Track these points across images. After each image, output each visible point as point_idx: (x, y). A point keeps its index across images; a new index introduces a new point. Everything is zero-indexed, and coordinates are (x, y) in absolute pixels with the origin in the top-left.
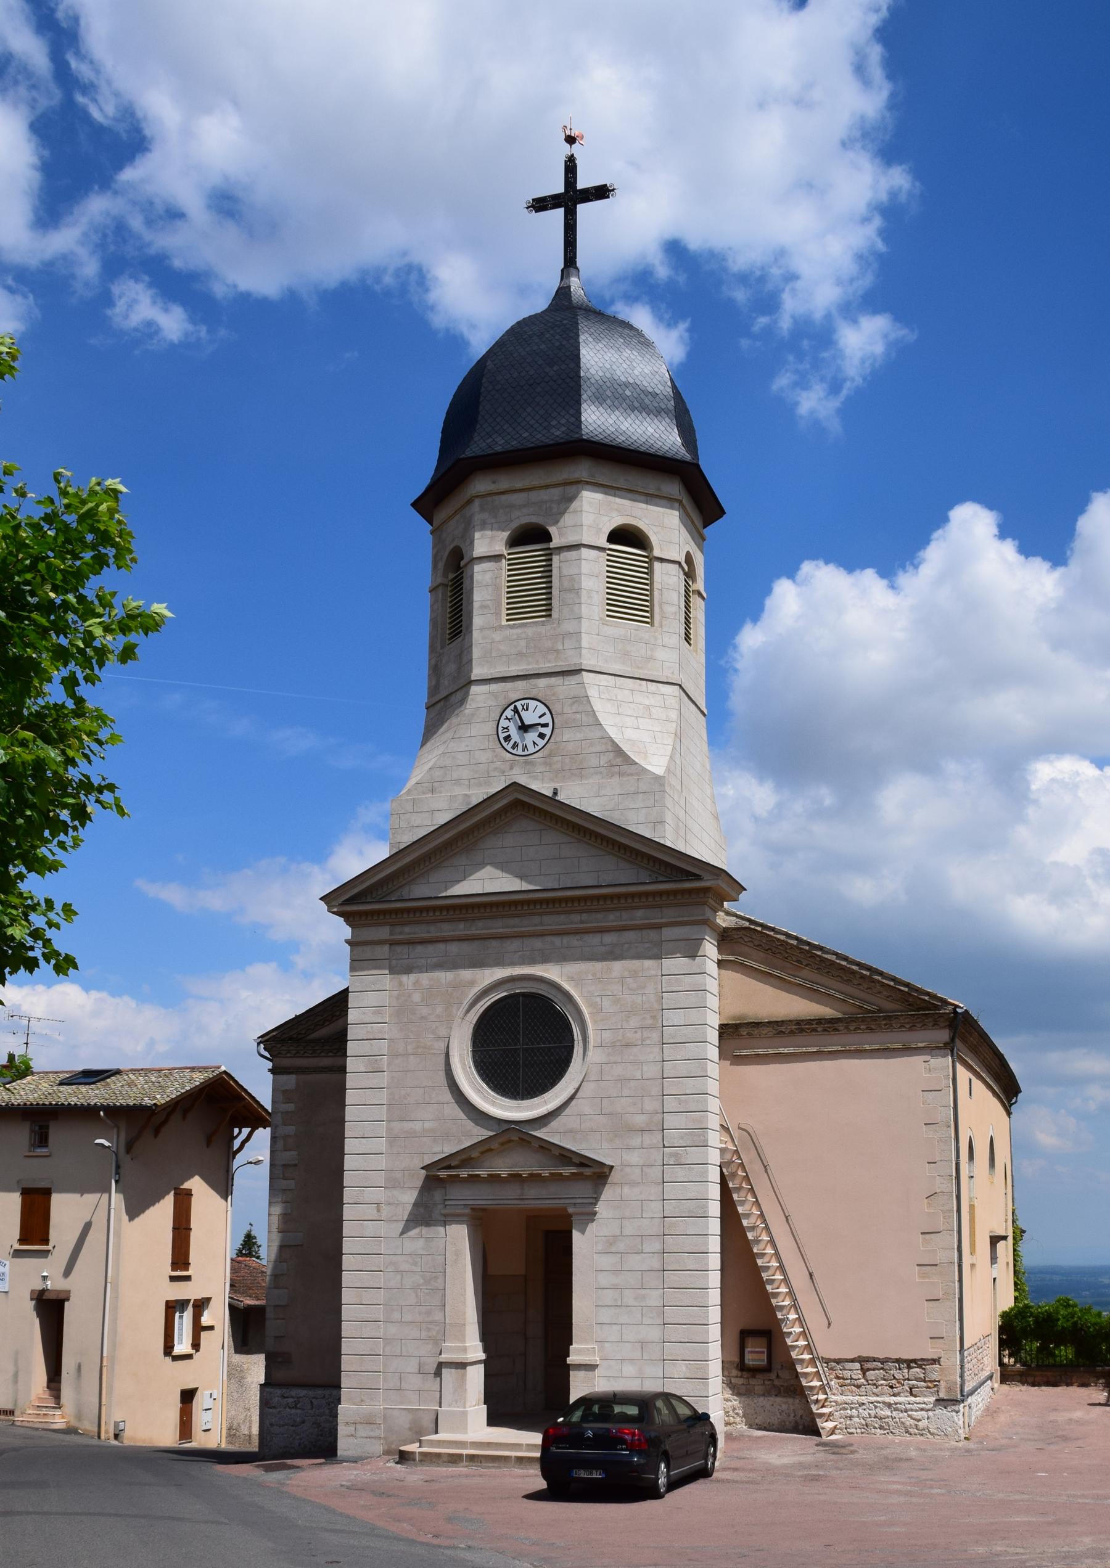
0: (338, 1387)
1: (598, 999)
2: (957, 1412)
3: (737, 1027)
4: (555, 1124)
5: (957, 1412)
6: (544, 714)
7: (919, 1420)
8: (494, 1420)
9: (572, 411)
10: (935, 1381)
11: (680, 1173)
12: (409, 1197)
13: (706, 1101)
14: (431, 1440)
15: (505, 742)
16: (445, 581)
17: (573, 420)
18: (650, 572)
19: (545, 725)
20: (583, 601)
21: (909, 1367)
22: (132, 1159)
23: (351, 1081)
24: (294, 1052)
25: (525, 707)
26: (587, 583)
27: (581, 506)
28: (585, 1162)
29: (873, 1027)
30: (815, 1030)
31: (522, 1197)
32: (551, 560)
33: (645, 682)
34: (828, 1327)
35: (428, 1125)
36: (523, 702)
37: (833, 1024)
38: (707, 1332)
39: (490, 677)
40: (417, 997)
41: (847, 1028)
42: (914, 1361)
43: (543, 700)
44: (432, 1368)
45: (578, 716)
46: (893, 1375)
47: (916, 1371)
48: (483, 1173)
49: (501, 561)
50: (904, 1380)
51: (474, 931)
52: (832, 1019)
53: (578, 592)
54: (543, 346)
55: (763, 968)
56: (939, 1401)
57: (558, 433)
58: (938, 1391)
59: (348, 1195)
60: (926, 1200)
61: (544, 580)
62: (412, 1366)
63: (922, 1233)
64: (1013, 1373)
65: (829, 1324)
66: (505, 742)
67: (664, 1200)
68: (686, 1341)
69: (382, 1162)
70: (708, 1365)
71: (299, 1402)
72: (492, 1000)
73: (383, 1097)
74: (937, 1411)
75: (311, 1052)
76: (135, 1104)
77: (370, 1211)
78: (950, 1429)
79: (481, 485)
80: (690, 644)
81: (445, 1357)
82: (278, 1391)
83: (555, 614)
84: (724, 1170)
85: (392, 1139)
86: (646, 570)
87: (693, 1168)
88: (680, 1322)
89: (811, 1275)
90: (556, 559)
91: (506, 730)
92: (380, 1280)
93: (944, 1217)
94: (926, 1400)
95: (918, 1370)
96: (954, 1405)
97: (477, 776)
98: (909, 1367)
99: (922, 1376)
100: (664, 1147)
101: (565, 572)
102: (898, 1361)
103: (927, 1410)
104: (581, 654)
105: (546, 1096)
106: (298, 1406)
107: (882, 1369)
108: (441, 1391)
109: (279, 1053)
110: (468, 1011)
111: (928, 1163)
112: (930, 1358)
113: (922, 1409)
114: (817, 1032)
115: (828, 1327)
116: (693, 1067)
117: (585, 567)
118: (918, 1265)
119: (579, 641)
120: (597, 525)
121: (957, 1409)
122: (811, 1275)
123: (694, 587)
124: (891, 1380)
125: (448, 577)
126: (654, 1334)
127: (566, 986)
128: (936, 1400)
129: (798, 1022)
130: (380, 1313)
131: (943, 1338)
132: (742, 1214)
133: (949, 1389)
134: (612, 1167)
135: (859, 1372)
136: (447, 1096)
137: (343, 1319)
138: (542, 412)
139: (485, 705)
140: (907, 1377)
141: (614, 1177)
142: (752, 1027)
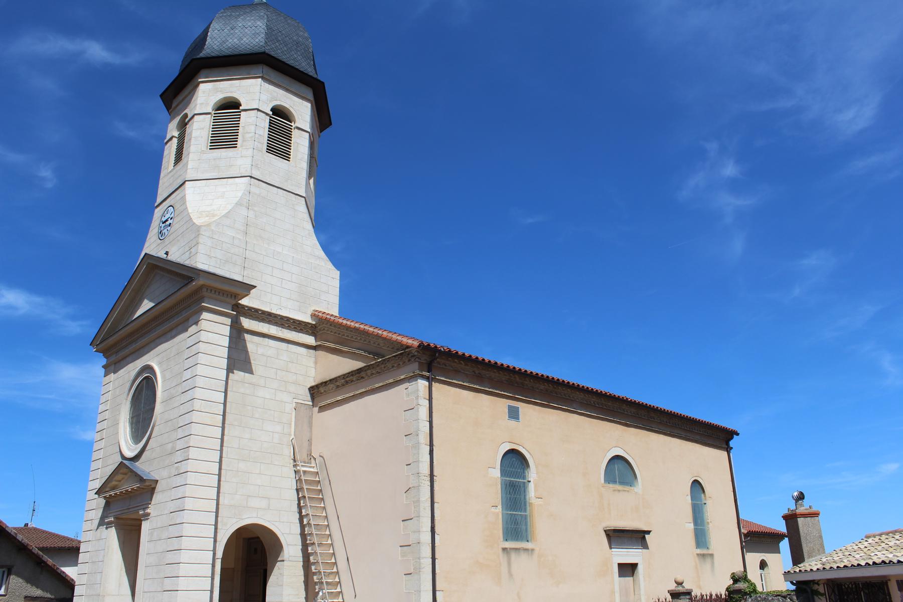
29: (379, 371)
30: (352, 381)
31: (129, 507)
52: (358, 370)
55: (332, 345)
60: (405, 494)
65: (356, 596)
93: (415, 508)
110: (128, 395)
111: (407, 465)
118: (401, 546)
141: (159, 487)
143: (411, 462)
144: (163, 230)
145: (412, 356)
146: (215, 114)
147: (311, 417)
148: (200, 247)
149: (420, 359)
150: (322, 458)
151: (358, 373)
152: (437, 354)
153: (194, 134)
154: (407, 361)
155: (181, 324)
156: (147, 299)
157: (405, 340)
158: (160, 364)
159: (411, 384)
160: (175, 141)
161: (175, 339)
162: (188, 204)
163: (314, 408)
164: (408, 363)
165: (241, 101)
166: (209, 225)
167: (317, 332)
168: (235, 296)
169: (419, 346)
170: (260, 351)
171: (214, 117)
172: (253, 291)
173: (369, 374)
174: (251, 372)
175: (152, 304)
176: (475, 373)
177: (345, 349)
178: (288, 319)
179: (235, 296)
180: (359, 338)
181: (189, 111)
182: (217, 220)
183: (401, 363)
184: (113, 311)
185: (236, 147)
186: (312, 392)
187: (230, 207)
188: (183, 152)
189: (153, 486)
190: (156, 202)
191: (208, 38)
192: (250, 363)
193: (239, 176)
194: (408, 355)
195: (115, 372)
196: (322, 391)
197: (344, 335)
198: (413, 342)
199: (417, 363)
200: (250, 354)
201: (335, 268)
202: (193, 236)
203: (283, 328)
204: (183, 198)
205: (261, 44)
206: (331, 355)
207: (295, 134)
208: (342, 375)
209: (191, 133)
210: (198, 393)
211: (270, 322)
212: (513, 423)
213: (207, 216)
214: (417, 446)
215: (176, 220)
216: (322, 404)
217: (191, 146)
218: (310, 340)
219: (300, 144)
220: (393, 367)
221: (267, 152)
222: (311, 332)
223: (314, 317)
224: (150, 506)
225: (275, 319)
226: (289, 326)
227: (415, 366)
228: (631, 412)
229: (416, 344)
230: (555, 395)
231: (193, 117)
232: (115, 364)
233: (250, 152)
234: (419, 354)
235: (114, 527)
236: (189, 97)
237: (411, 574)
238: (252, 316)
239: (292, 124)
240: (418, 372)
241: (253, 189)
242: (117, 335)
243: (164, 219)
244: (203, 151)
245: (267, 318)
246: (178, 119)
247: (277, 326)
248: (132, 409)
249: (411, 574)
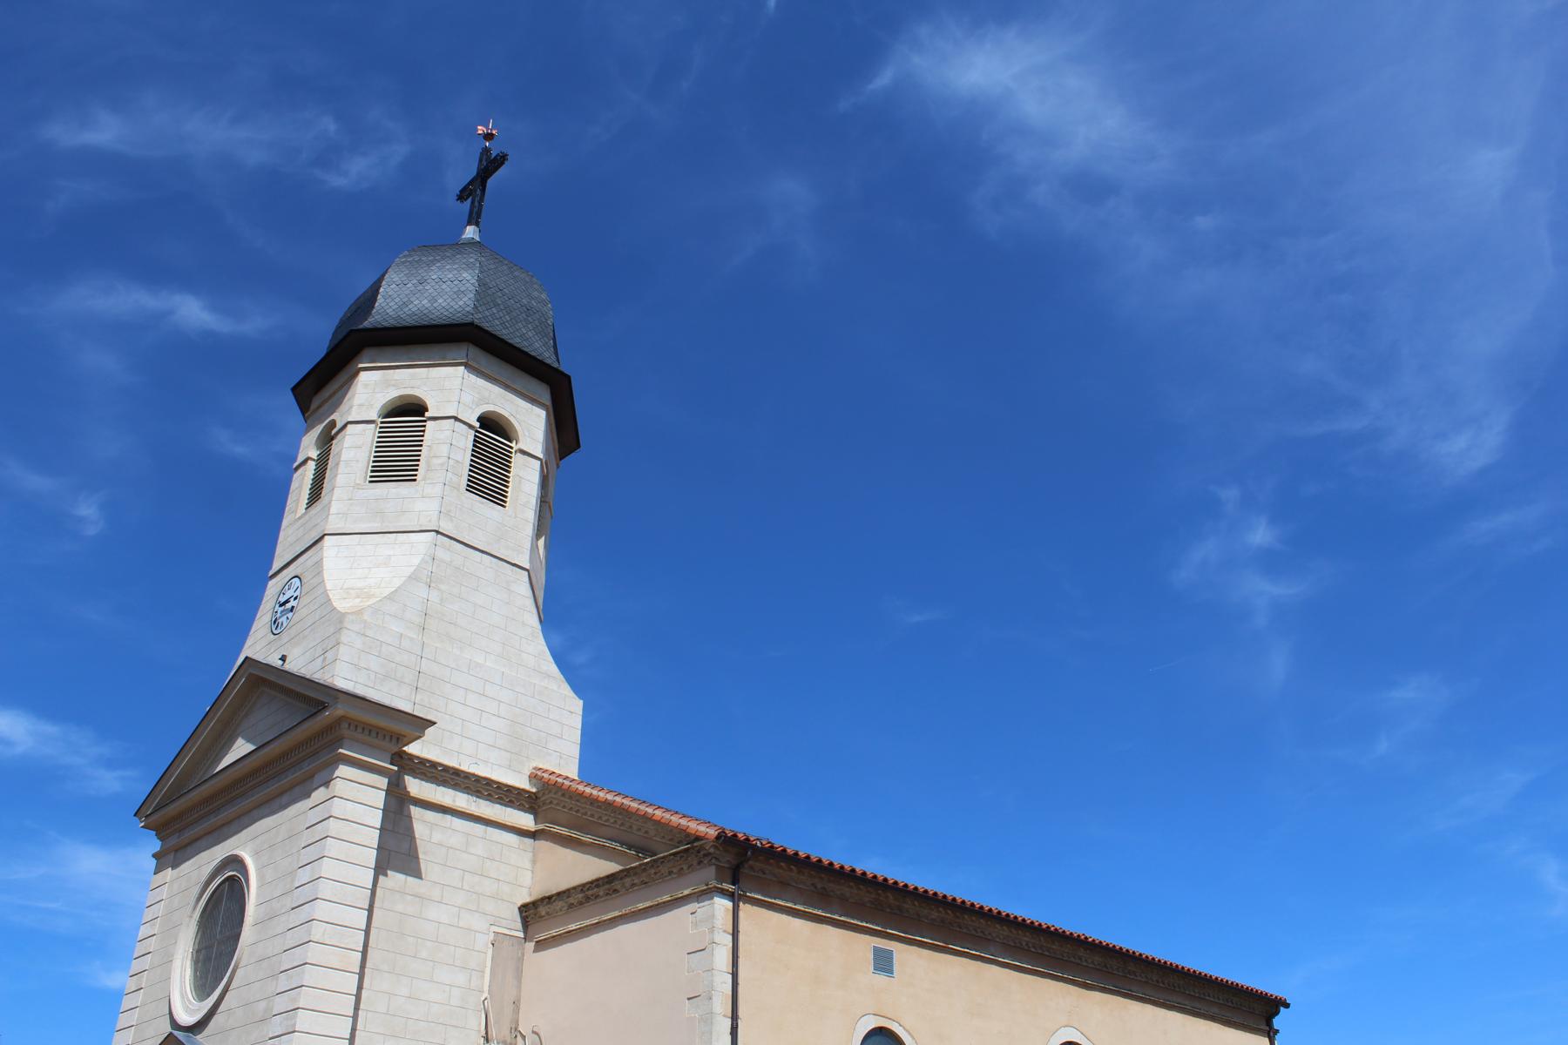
29: (646, 880)
30: (597, 897)
52: (608, 877)
55: (564, 831)
110: (195, 908)
144: (280, 617)
145: (705, 855)
146: (382, 423)
147: (521, 960)
148: (342, 649)
149: (720, 862)
150: (536, 1036)
151: (608, 883)
152: (749, 853)
153: (345, 455)
154: (695, 863)
155: (297, 785)
156: (243, 738)
157: (694, 826)
158: (256, 854)
160: (311, 465)
162: (326, 575)
163: (527, 943)
164: (698, 867)
165: (428, 403)
166: (360, 612)
167: (539, 806)
168: (398, 739)
169: (718, 837)
170: (437, 836)
171: (381, 428)
172: (430, 731)
173: (627, 885)
174: (416, 873)
175: (250, 747)
176: (816, 887)
177: (586, 838)
178: (489, 782)
179: (398, 739)
180: (612, 821)
181: (339, 417)
182: (374, 604)
184: (179, 759)
185: (415, 480)
186: (524, 914)
187: (397, 583)
188: (324, 485)
190: (271, 568)
191: (379, 297)
192: (417, 858)
194: (699, 852)
195: (174, 867)
196: (543, 913)
197: (586, 814)
198: (708, 830)
199: (714, 867)
200: (418, 841)
201: (575, 696)
202: (332, 630)
203: (478, 797)
204: (319, 563)
205: (467, 309)
206: (560, 848)
207: (517, 460)
208: (579, 886)
209: (339, 454)
210: (321, 910)
211: (456, 786)
212: (881, 979)
213: (358, 597)
214: (708, 1018)
215: (304, 601)
216: (542, 936)
217: (339, 476)
218: (526, 821)
219: (525, 478)
220: (670, 873)
221: (467, 490)
222: (527, 806)
223: (534, 781)
225: (466, 781)
226: (489, 795)
228: (1093, 962)
229: (712, 833)
230: (958, 929)
231: (345, 426)
232: (176, 851)
233: (438, 489)
234: (718, 852)
236: (337, 396)
238: (426, 776)
239: (513, 445)
240: (713, 883)
241: (440, 553)
242: (183, 800)
243: (282, 599)
244: (359, 484)
245: (452, 779)
246: (319, 429)
247: (468, 794)
248: (199, 934)
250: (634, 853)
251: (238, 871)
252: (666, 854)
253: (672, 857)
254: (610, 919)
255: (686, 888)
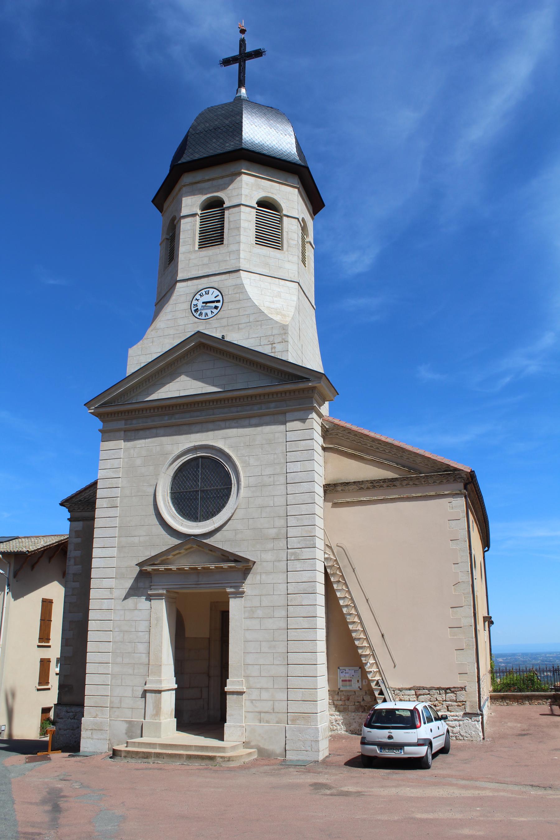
0: (82, 705)
1: (247, 458)
2: (478, 722)
3: (335, 485)
4: (218, 535)
5: (478, 722)
6: (218, 296)
7: (454, 727)
8: (181, 727)
9: (237, 139)
10: (463, 701)
11: (298, 565)
12: (128, 583)
13: (314, 518)
14: (134, 742)
15: (195, 312)
16: (168, 237)
17: (238, 142)
18: (281, 221)
19: (218, 301)
20: (241, 233)
21: (446, 693)
22: (17, 581)
23: (98, 513)
24: (82, 508)
25: (207, 293)
26: (243, 224)
27: (242, 185)
28: (237, 559)
29: (417, 483)
30: (381, 486)
31: (198, 583)
32: (224, 212)
33: (278, 279)
34: (394, 668)
35: (142, 539)
36: (206, 290)
37: (393, 482)
38: (316, 669)
39: (187, 278)
40: (138, 462)
41: (401, 484)
42: (449, 689)
43: (217, 288)
44: (140, 693)
45: (238, 295)
46: (436, 698)
47: (451, 696)
48: (174, 568)
49: (196, 216)
50: (443, 701)
51: (173, 421)
52: (392, 479)
53: (239, 229)
54: (223, 112)
55: (350, 451)
56: (466, 714)
57: (229, 146)
58: (465, 708)
59: (94, 583)
61: (220, 223)
62: (128, 693)
63: (451, 608)
64: (497, 697)
66: (195, 312)
67: (287, 583)
68: (303, 675)
69: (114, 562)
70: (317, 692)
71: (76, 715)
72: (183, 461)
73: (117, 522)
74: (465, 721)
75: (91, 508)
76: (17, 551)
77: (106, 594)
78: (474, 733)
79: (187, 179)
80: (305, 266)
81: (148, 687)
82: (65, 709)
83: (225, 242)
84: (329, 571)
85: (121, 548)
86: (279, 220)
87: (306, 561)
88: (298, 663)
89: (383, 636)
90: (226, 213)
91: (195, 306)
92: (110, 636)
93: (465, 598)
94: (457, 714)
95: (452, 694)
96: (476, 717)
97: (178, 332)
98: (446, 693)
99: (454, 698)
100: (288, 548)
101: (231, 219)
102: (439, 689)
103: (459, 721)
104: (240, 262)
105: (215, 519)
106: (75, 718)
107: (429, 694)
108: (145, 709)
109: (74, 509)
112: (459, 686)
113: (455, 720)
114: (384, 487)
115: (394, 668)
116: (306, 498)
117: (243, 216)
118: (449, 628)
119: (239, 255)
120: (251, 195)
121: (478, 720)
122: (383, 636)
123: (307, 240)
124: (435, 701)
125: (169, 235)
126: (282, 670)
127: (227, 450)
128: (464, 714)
129: (372, 482)
130: (109, 658)
131: (467, 673)
132: (336, 590)
133: (472, 707)
134: (255, 562)
135: (414, 696)
136: (155, 521)
137: (87, 661)
138: (221, 141)
139: (184, 293)
140: (445, 699)
142: (344, 486)
143: (459, 562)
145: (459, 478)
151: (391, 481)
159: (456, 499)
161: (259, 429)
183: (445, 481)
189: (252, 567)
193: (290, 280)
194: (456, 476)
220: (434, 482)
221: (256, 243)
224: (244, 585)
227: (461, 486)
235: (164, 600)
237: (463, 649)
249: (463, 649)
250: (407, 469)
251: (211, 454)
252: (435, 474)
253: (439, 476)
254: (391, 498)
255: (446, 491)
